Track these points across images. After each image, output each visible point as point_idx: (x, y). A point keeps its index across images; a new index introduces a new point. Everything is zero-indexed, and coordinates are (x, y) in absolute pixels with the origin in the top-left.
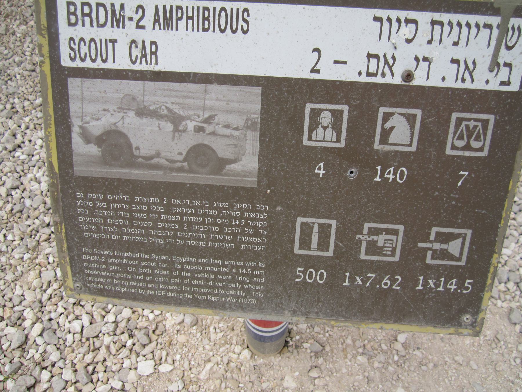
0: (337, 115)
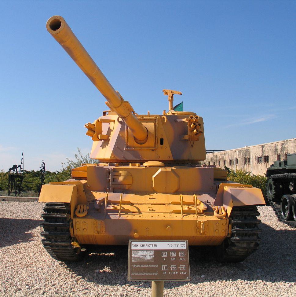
0: (166, 253)
